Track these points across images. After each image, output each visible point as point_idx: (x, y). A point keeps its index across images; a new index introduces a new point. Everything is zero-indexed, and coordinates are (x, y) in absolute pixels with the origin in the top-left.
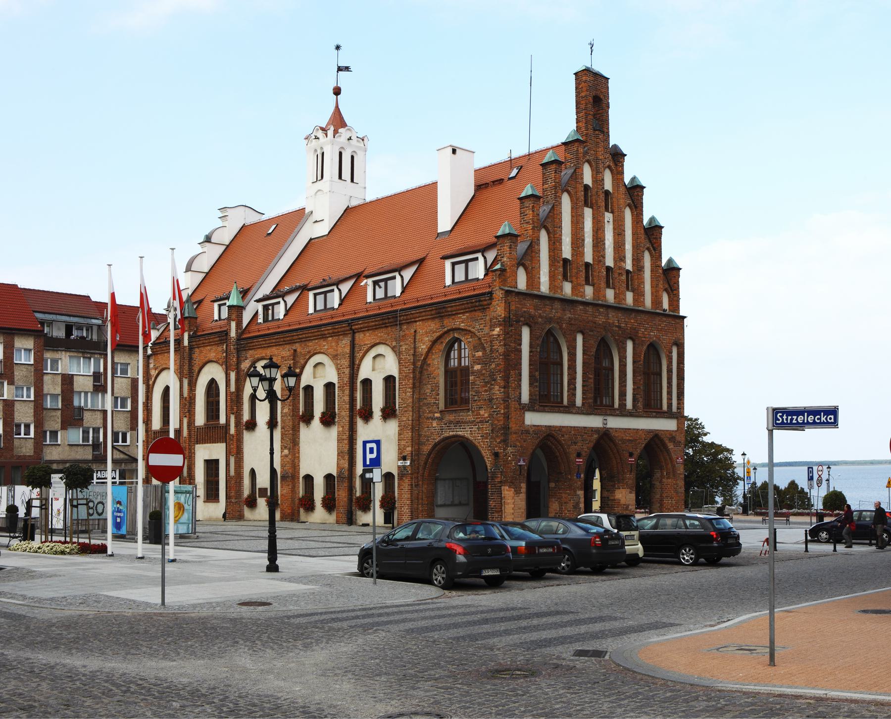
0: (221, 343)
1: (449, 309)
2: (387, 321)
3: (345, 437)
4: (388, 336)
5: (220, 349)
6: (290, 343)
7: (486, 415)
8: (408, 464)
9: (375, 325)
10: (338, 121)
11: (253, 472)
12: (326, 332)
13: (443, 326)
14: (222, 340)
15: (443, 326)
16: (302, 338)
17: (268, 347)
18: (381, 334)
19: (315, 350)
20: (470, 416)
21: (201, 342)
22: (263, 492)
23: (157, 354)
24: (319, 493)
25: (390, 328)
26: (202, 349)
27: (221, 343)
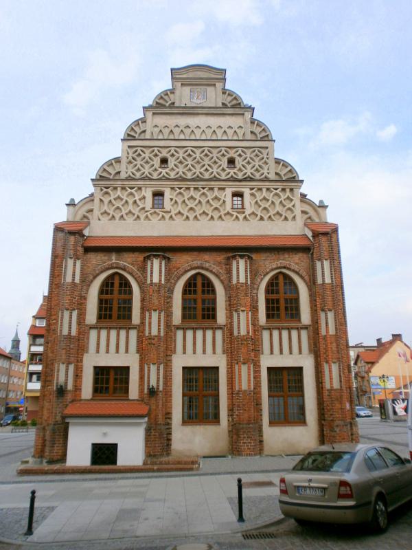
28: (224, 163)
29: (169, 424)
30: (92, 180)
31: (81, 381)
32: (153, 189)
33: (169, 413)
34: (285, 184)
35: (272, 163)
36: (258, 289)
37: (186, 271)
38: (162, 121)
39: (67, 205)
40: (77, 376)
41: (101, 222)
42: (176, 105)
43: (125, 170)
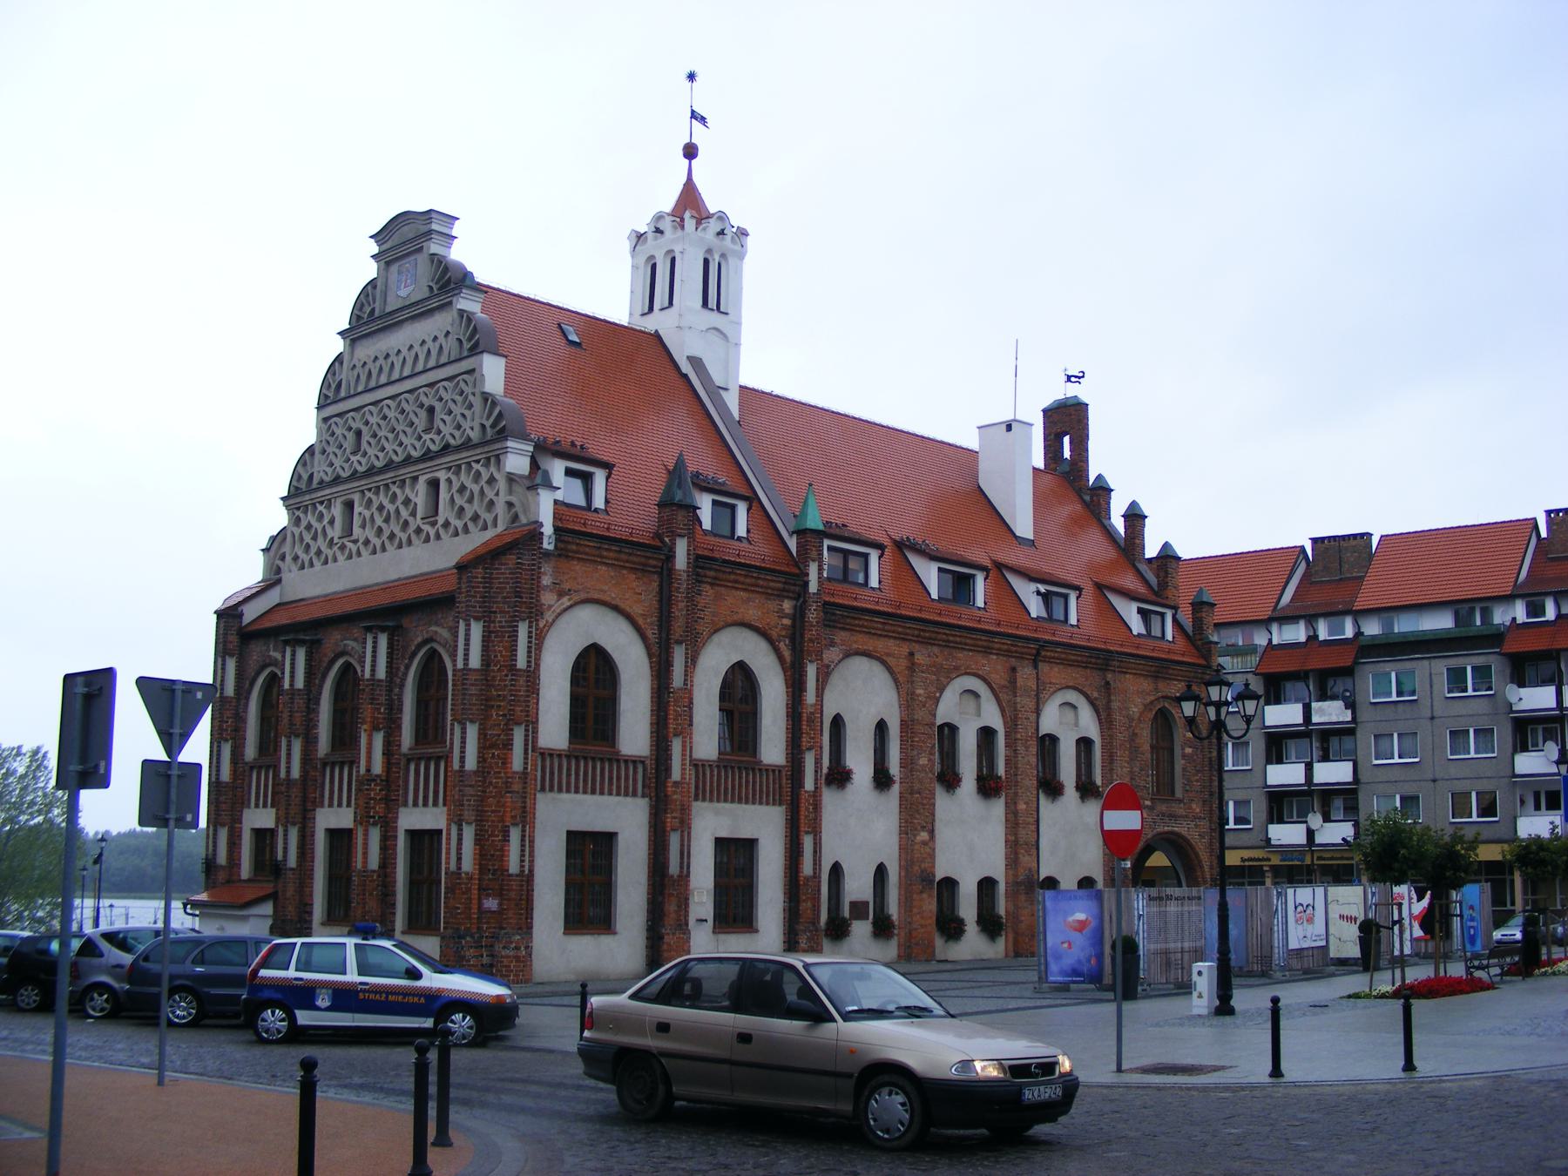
0: (781, 595)
1: (1171, 671)
2: (1093, 660)
3: (1031, 820)
4: (1086, 680)
5: (772, 605)
6: (922, 642)
7: (1198, 810)
8: (1129, 866)
9: (1074, 661)
10: (689, 197)
11: (836, 870)
12: (997, 646)
13: (1156, 689)
14: (788, 591)
15: (1156, 689)
16: (949, 641)
17: (881, 635)
18: (1076, 675)
19: (968, 667)
20: (1180, 810)
21: (732, 577)
22: (859, 909)
23: (573, 558)
24: (968, 909)
25: (1088, 671)
26: (723, 590)
27: (778, 596)
28: (421, 421)
29: (310, 922)
30: (282, 499)
31: (240, 852)
32: (344, 498)
33: (306, 904)
34: (486, 449)
35: (477, 402)
36: (402, 686)
37: (332, 662)
38: (366, 350)
39: (263, 550)
40: (234, 844)
41: (292, 575)
42: (377, 314)
43: (321, 470)
